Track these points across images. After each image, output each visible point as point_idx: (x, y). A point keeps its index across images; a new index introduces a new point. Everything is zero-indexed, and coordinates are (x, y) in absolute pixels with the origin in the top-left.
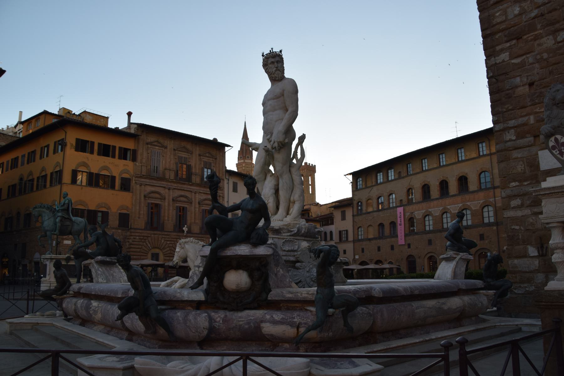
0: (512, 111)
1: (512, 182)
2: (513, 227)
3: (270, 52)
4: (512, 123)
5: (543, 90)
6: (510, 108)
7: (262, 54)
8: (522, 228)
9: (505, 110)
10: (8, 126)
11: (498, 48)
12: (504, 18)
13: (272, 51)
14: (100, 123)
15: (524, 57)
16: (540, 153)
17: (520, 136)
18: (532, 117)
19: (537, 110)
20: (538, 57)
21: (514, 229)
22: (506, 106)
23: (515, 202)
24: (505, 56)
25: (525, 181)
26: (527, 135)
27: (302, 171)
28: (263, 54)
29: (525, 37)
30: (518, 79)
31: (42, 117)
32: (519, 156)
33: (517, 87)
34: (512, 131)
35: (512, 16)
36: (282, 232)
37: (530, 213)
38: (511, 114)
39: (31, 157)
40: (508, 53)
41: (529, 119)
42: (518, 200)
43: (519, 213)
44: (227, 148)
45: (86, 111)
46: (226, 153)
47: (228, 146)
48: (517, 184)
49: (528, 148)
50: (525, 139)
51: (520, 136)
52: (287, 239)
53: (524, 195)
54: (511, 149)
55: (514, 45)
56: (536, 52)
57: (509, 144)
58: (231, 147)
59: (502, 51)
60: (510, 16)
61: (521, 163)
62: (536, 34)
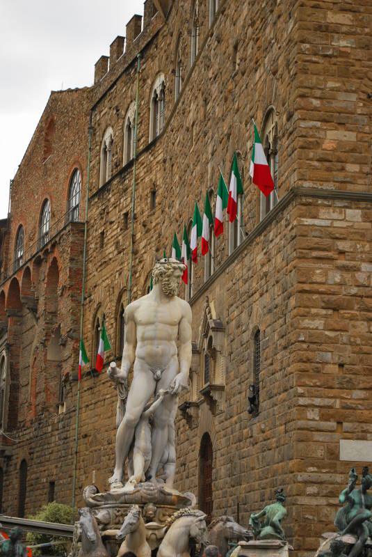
0: (319, 389)
1: (311, 466)
2: (306, 516)
4: (317, 401)
5: (353, 376)
6: (318, 384)
8: (316, 519)
9: (312, 384)
11: (314, 311)
12: (323, 280)
15: (338, 333)
16: (342, 442)
17: (324, 418)
18: (338, 401)
19: (344, 395)
20: (352, 339)
21: (307, 518)
22: (314, 381)
23: (312, 489)
24: (319, 323)
25: (324, 468)
26: (331, 420)
29: (342, 312)
30: (329, 355)
32: (321, 440)
33: (327, 363)
34: (317, 410)
35: (332, 283)
37: (325, 503)
38: (318, 391)
40: (323, 322)
41: (335, 402)
42: (315, 487)
43: (314, 502)
48: (315, 469)
49: (330, 433)
50: (329, 423)
51: (324, 418)
53: (321, 483)
54: (312, 429)
55: (331, 315)
56: (349, 334)
57: (311, 423)
59: (317, 315)
60: (330, 282)
61: (322, 448)
62: (352, 314)
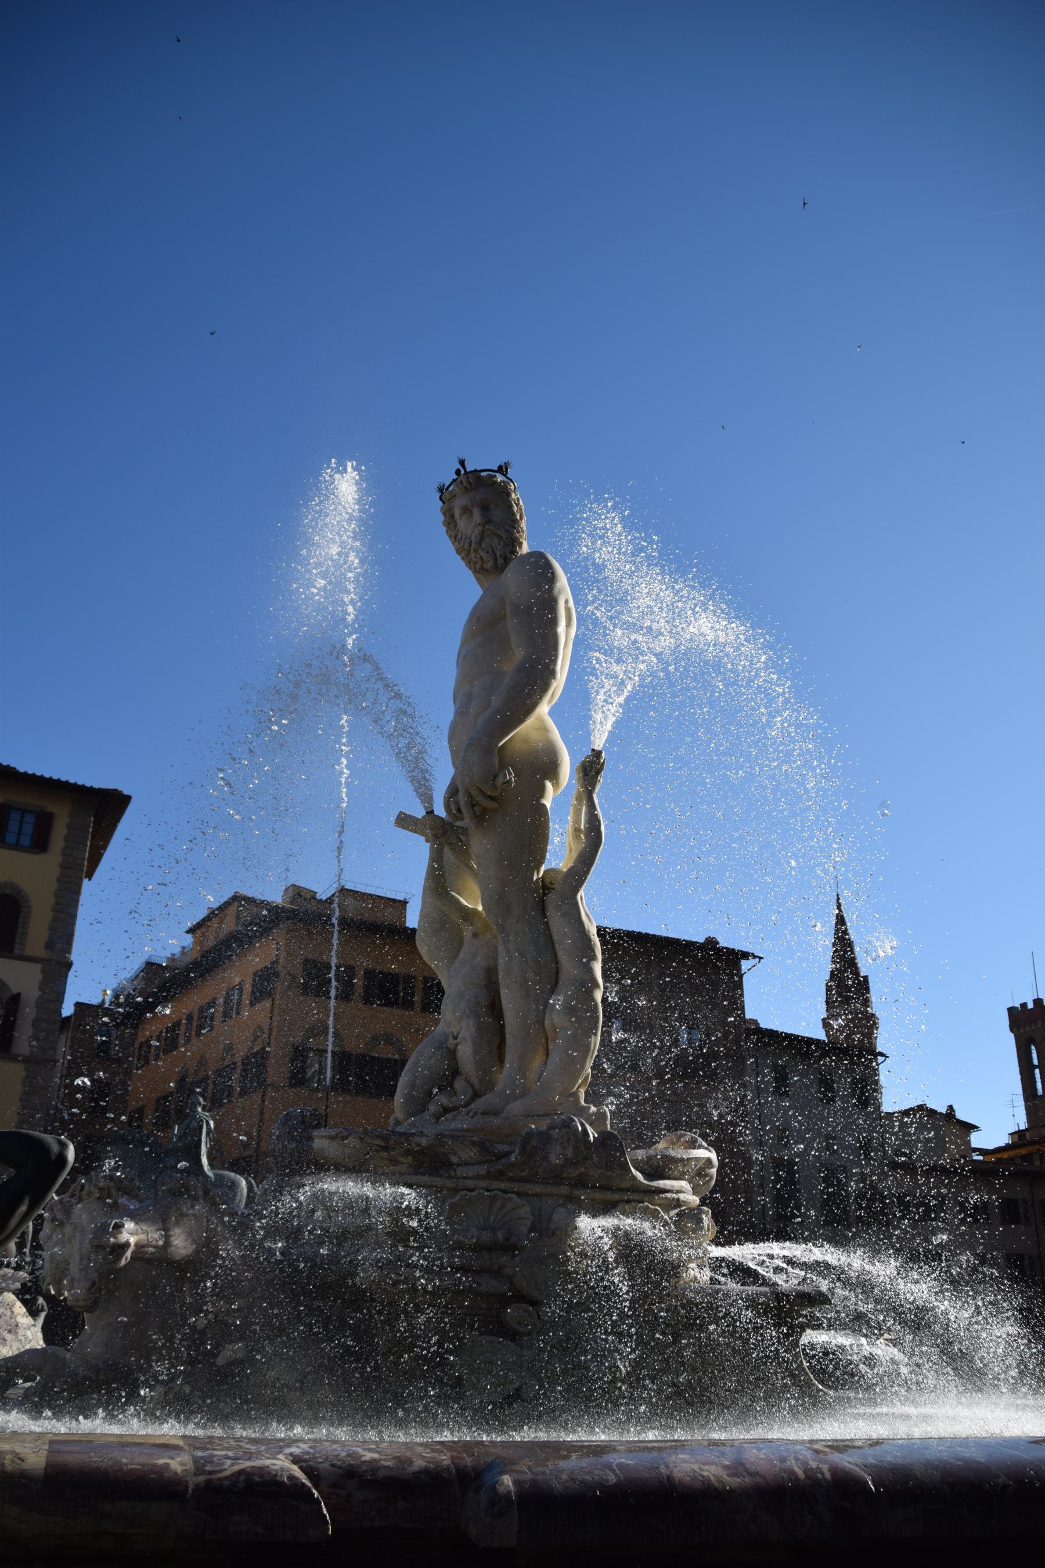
3: (455, 477)
7: (439, 494)
10: (183, 948)
13: (463, 472)
14: (388, 916)
27: (1030, 1026)
28: (441, 490)
31: (232, 910)
36: (454, 1159)
39: (202, 1019)
44: (745, 965)
45: (346, 887)
46: (746, 979)
47: (745, 955)
52: (472, 1190)
58: (758, 959)
